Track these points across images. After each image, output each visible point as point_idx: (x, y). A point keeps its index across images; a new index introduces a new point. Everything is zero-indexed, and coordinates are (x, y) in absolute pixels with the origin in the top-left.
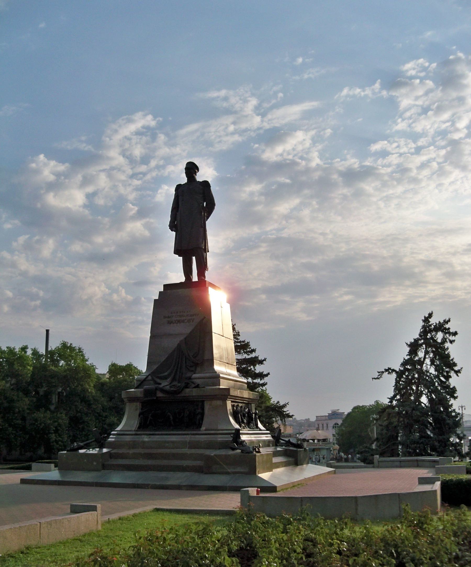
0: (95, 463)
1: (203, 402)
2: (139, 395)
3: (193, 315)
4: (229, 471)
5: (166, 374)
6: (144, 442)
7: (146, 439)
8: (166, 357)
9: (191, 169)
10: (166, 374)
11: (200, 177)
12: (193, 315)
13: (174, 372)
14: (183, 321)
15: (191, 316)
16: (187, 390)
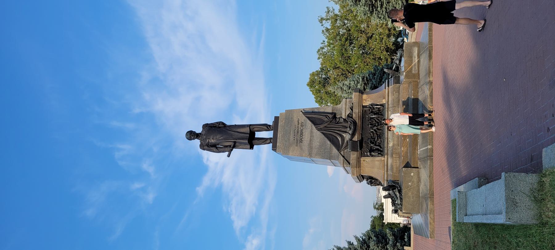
0: (412, 174)
1: (364, 107)
2: (355, 156)
3: (298, 122)
4: (417, 61)
5: (340, 139)
6: (394, 145)
7: (391, 145)
8: (326, 139)
9: (192, 135)
10: (340, 139)
11: (199, 130)
12: (298, 122)
13: (338, 132)
14: (302, 130)
15: (298, 124)
16: (354, 116)
